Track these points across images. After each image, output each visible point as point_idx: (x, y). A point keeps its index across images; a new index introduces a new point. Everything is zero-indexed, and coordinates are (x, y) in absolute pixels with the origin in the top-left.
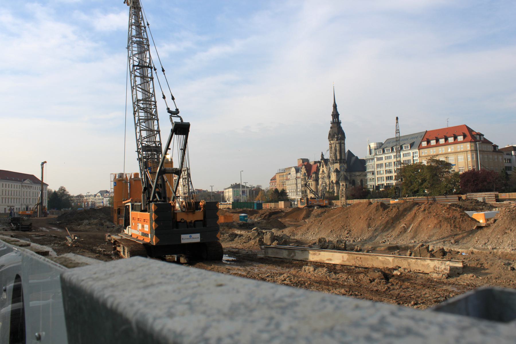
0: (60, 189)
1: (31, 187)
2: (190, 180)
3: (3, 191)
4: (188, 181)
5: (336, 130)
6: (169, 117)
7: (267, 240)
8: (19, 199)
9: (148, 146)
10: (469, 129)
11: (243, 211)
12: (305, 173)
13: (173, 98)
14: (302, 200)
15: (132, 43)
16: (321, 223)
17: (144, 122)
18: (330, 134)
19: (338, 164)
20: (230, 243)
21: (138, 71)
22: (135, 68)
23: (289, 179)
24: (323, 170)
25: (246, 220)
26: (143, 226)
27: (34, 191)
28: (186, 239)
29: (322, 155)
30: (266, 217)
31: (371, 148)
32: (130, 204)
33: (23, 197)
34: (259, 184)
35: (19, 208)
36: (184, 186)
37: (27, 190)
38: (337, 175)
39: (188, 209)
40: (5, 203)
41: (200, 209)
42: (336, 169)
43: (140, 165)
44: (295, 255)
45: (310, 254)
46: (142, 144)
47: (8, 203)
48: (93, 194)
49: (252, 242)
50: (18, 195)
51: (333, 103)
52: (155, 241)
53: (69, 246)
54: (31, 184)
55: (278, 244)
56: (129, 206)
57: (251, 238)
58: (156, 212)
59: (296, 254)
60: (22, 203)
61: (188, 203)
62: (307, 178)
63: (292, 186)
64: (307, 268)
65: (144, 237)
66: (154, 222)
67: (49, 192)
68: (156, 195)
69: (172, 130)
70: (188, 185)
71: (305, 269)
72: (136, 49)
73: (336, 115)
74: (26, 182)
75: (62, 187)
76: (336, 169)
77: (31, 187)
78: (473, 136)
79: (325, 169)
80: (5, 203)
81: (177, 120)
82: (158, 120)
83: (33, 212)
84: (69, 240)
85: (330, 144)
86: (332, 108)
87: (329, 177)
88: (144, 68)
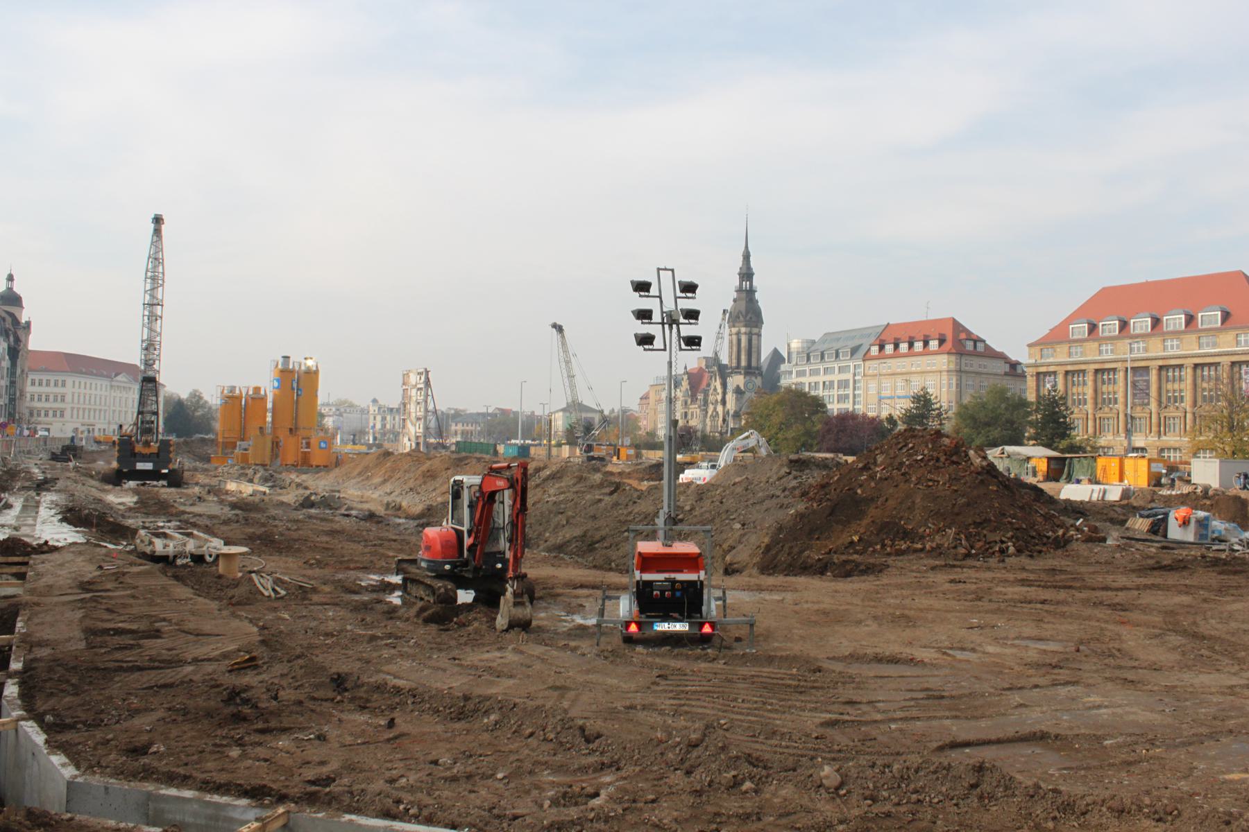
1: (130, 388)
2: (430, 393)
4: (427, 395)
5: (742, 306)
8: (105, 411)
10: (957, 326)
28: (140, 466)
31: (792, 350)
33: (112, 408)
38: (737, 399)
42: (738, 386)
50: (103, 403)
51: (743, 248)
70: (426, 402)
73: (747, 274)
74: (119, 378)
75: (195, 391)
76: (738, 386)
77: (130, 388)
78: (958, 343)
87: (724, 402)
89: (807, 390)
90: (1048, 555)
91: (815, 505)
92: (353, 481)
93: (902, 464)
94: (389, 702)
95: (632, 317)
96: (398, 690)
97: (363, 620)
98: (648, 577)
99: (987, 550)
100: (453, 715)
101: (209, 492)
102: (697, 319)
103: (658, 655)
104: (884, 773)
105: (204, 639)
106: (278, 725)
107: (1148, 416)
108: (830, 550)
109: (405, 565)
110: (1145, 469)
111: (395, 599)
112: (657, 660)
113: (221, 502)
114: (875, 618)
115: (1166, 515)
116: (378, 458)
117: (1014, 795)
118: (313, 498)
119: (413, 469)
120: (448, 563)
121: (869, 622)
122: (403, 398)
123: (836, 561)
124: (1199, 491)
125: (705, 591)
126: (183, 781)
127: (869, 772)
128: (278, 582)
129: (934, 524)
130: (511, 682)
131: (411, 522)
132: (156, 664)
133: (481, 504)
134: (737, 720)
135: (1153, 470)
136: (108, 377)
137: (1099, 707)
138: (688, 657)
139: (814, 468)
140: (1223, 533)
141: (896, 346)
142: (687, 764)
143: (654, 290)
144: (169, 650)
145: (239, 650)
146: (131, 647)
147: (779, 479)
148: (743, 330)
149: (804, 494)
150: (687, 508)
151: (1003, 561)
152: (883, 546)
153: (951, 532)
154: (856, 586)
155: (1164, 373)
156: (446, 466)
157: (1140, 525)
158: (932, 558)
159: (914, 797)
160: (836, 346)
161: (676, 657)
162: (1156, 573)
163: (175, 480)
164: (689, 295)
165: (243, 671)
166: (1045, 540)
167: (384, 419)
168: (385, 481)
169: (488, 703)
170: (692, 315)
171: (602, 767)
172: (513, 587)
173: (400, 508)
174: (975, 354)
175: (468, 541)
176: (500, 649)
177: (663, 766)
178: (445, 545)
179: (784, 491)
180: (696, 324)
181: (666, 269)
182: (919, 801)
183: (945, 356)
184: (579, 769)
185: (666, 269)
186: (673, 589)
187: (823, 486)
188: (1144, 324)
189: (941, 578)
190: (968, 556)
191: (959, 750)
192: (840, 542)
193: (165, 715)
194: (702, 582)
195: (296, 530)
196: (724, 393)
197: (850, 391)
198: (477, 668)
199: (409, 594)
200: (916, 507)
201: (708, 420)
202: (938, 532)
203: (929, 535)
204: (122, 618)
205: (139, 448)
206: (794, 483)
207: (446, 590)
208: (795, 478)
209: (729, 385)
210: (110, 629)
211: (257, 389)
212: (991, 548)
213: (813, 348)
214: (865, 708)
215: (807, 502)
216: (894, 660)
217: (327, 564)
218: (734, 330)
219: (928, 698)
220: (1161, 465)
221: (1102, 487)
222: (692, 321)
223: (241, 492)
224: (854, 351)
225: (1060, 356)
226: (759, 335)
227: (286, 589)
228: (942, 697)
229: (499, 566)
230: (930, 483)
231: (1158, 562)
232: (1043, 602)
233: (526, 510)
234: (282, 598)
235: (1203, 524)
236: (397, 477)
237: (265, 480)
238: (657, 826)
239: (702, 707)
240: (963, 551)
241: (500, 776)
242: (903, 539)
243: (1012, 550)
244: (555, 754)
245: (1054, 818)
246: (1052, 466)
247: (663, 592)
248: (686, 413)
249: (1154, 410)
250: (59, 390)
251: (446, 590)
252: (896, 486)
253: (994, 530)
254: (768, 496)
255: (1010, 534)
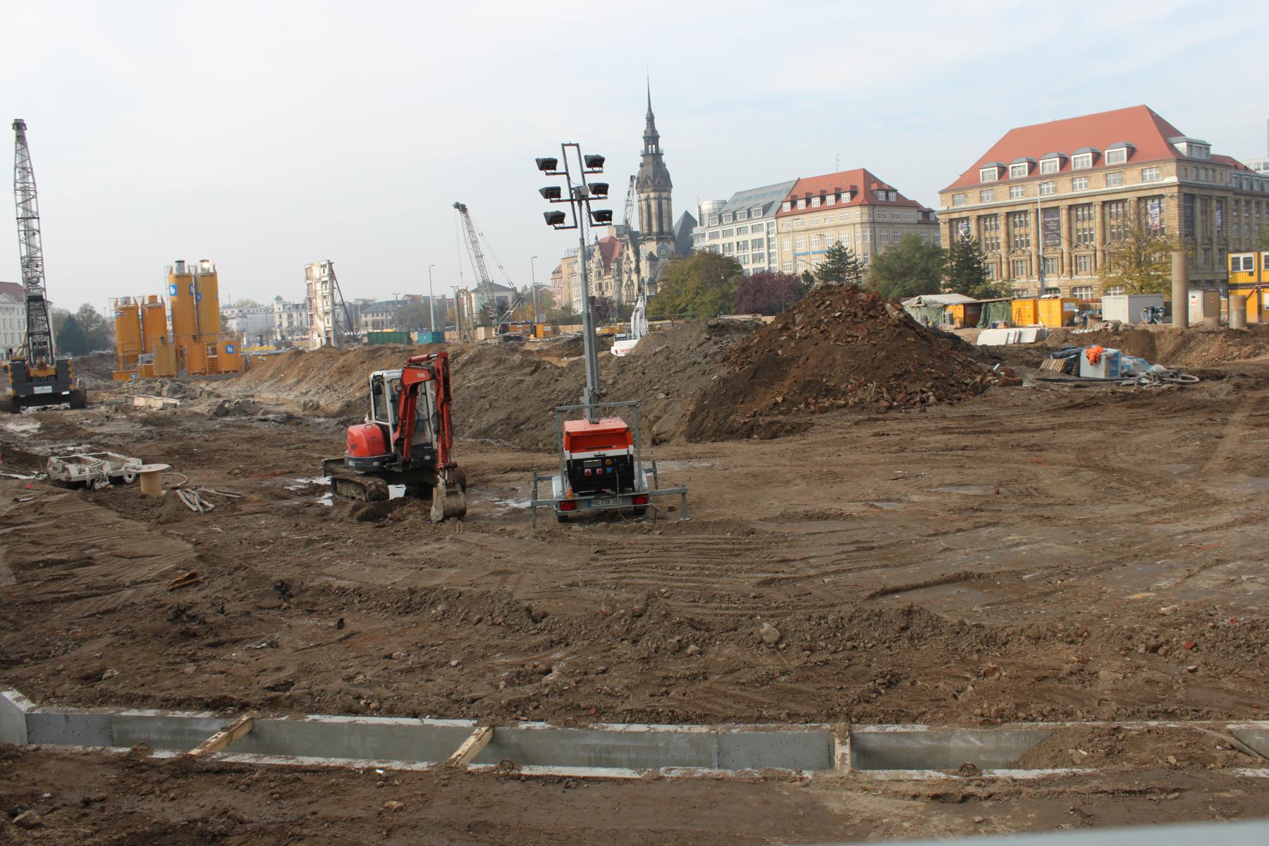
0: (81, 308)
1: (13, 309)
2: (335, 286)
10: (867, 175)
19: (654, 243)
28: (38, 390)
36: (325, 297)
42: (651, 253)
51: (646, 111)
62: (603, 271)
70: (332, 295)
73: (652, 137)
76: (651, 253)
77: (13, 309)
86: (645, 121)
87: (638, 270)
89: (721, 252)
90: (967, 402)
91: (737, 369)
92: (267, 384)
93: (820, 322)
94: (336, 604)
95: (541, 196)
96: (343, 591)
97: (297, 525)
98: (577, 456)
99: (908, 401)
100: (400, 610)
101: (117, 410)
102: (606, 193)
103: (595, 532)
104: (819, 624)
105: (139, 561)
106: (229, 637)
107: (1060, 256)
108: (755, 413)
109: (332, 466)
110: (1058, 309)
111: (326, 500)
112: (594, 536)
113: (131, 419)
114: (803, 477)
115: (1078, 354)
116: (289, 358)
117: (941, 633)
118: (227, 405)
119: (328, 366)
120: (376, 460)
121: (798, 481)
122: (308, 293)
123: (762, 423)
124: (1110, 327)
125: (636, 464)
126: (144, 701)
127: (806, 625)
128: (205, 495)
129: (855, 379)
130: (453, 571)
131: (331, 420)
132: (94, 591)
133: (404, 397)
134: (677, 587)
135: (1066, 310)
137: (1018, 545)
138: (624, 531)
139: (733, 331)
140: (1132, 368)
141: (808, 202)
142: (632, 635)
143: (560, 167)
144: (105, 576)
145: (177, 569)
146: (65, 577)
147: (700, 345)
148: (652, 195)
149: (725, 359)
150: (610, 382)
151: (924, 411)
152: (807, 404)
153: (872, 386)
154: (783, 447)
155: (1073, 212)
156: (361, 360)
157: (1054, 365)
158: (855, 413)
159: (849, 644)
160: (748, 205)
161: (611, 532)
162: (1070, 412)
163: (78, 401)
164: (596, 169)
165: (184, 589)
166: (964, 387)
167: (290, 316)
168: (299, 382)
169: (434, 594)
170: (601, 189)
171: (552, 645)
172: (444, 477)
173: (318, 407)
174: (887, 204)
175: (393, 436)
176: (438, 540)
177: (610, 638)
178: (371, 442)
179: (705, 357)
180: (606, 198)
181: (570, 145)
182: (854, 647)
183: (858, 209)
184: (530, 648)
185: (570, 145)
186: (604, 466)
187: (744, 350)
188: (1053, 164)
189: (865, 432)
190: (890, 408)
191: (890, 597)
192: (764, 404)
193: (113, 639)
194: (631, 457)
195: (214, 440)
196: (638, 261)
197: (764, 250)
198: (417, 561)
199: (339, 494)
200: (837, 363)
201: (623, 289)
202: (860, 387)
203: (851, 391)
204: (50, 549)
205: (34, 372)
206: (715, 348)
207: (377, 487)
208: (716, 343)
209: (641, 252)
210: (39, 562)
211: (153, 298)
212: (912, 399)
213: (724, 209)
214: (798, 564)
215: (729, 367)
216: (824, 517)
217: (252, 472)
218: (643, 196)
219: (858, 550)
220: (1074, 304)
221: (1017, 330)
222: (601, 196)
223: (150, 407)
224: (766, 209)
225: (972, 201)
226: (669, 199)
227: (213, 502)
228: (872, 548)
229: (428, 458)
230: (850, 339)
231: (1071, 401)
232: (964, 448)
233: (450, 400)
234: (211, 511)
235: (1112, 360)
236: (312, 375)
237: (173, 392)
238: (610, 694)
239: (642, 578)
240: (885, 404)
241: (454, 663)
242: (826, 396)
243: (932, 399)
244: (504, 637)
245: (979, 651)
246: (969, 313)
247: (594, 470)
248: (600, 284)
249: (1065, 251)
251: (377, 487)
252: (816, 344)
253: (914, 381)
254: (689, 364)
255: (930, 383)
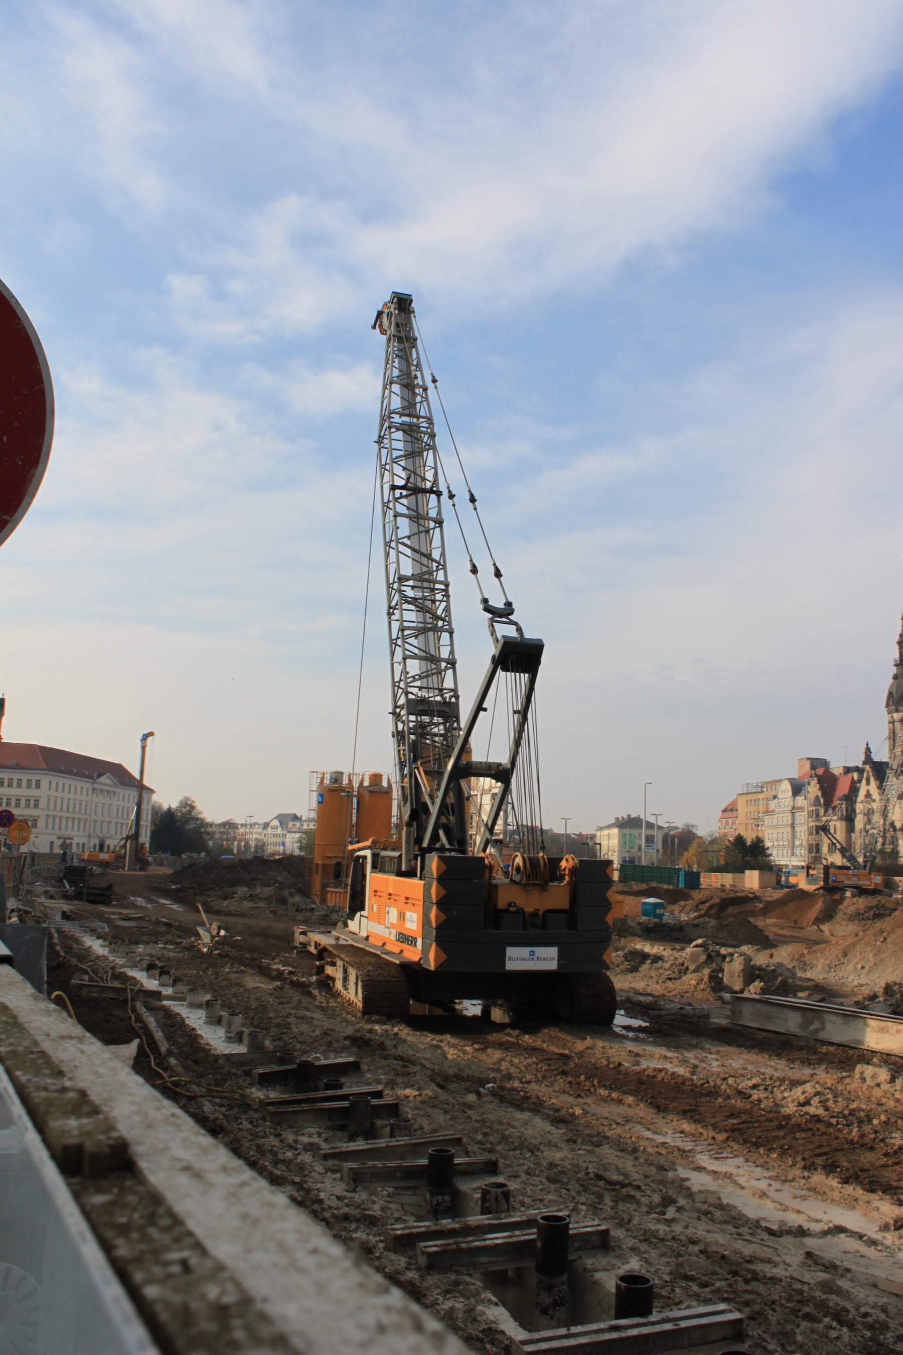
0: (181, 802)
1: (115, 793)
3: (49, 800)
6: (486, 624)
7: (732, 975)
8: (86, 820)
9: (423, 701)
11: (648, 889)
12: (817, 796)
13: (498, 574)
14: (811, 871)
15: (390, 427)
16: (885, 939)
17: (416, 637)
18: (890, 695)
20: (629, 977)
21: (404, 501)
22: (398, 493)
23: (773, 811)
24: (868, 791)
25: (660, 916)
26: (402, 916)
27: (121, 803)
29: (868, 750)
30: (713, 912)
32: (368, 853)
33: (94, 817)
34: (691, 822)
35: (84, 844)
37: (103, 801)
39: (528, 878)
40: (53, 828)
41: (561, 878)
43: (399, 751)
44: (823, 1028)
45: (868, 1029)
46: (407, 693)
47: (60, 829)
48: (262, 821)
49: (690, 979)
52: (435, 960)
53: (202, 953)
54: (115, 785)
55: (764, 991)
56: (365, 858)
57: (687, 969)
58: (442, 879)
59: (828, 1026)
60: (92, 831)
61: (530, 859)
62: (822, 811)
63: (781, 830)
64: (869, 1070)
65: (404, 946)
66: (434, 908)
67: (156, 811)
68: (441, 833)
69: (494, 657)
71: (862, 1073)
72: (400, 445)
74: (103, 779)
75: (187, 799)
77: (115, 793)
79: (873, 787)
80: (53, 828)
81: (506, 630)
82: (451, 633)
83: (114, 855)
84: (206, 937)
85: (890, 723)
88: (420, 495)
136: (90, 777)
250: (33, 792)
